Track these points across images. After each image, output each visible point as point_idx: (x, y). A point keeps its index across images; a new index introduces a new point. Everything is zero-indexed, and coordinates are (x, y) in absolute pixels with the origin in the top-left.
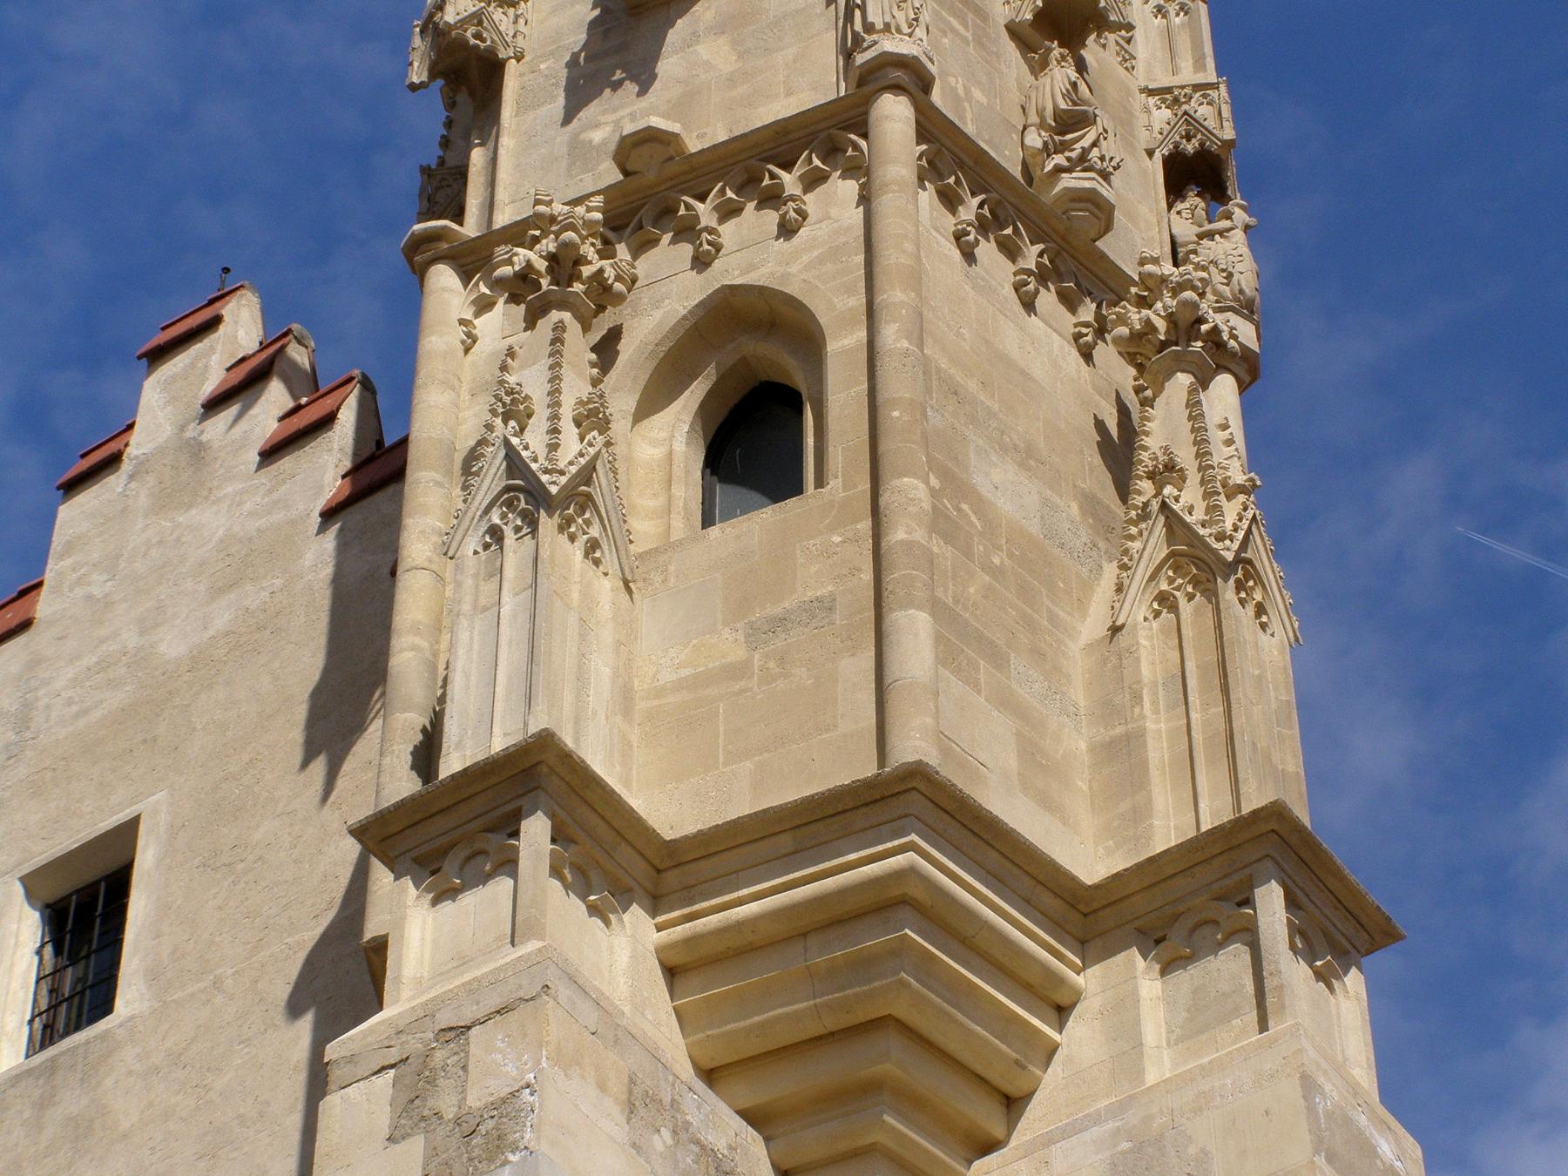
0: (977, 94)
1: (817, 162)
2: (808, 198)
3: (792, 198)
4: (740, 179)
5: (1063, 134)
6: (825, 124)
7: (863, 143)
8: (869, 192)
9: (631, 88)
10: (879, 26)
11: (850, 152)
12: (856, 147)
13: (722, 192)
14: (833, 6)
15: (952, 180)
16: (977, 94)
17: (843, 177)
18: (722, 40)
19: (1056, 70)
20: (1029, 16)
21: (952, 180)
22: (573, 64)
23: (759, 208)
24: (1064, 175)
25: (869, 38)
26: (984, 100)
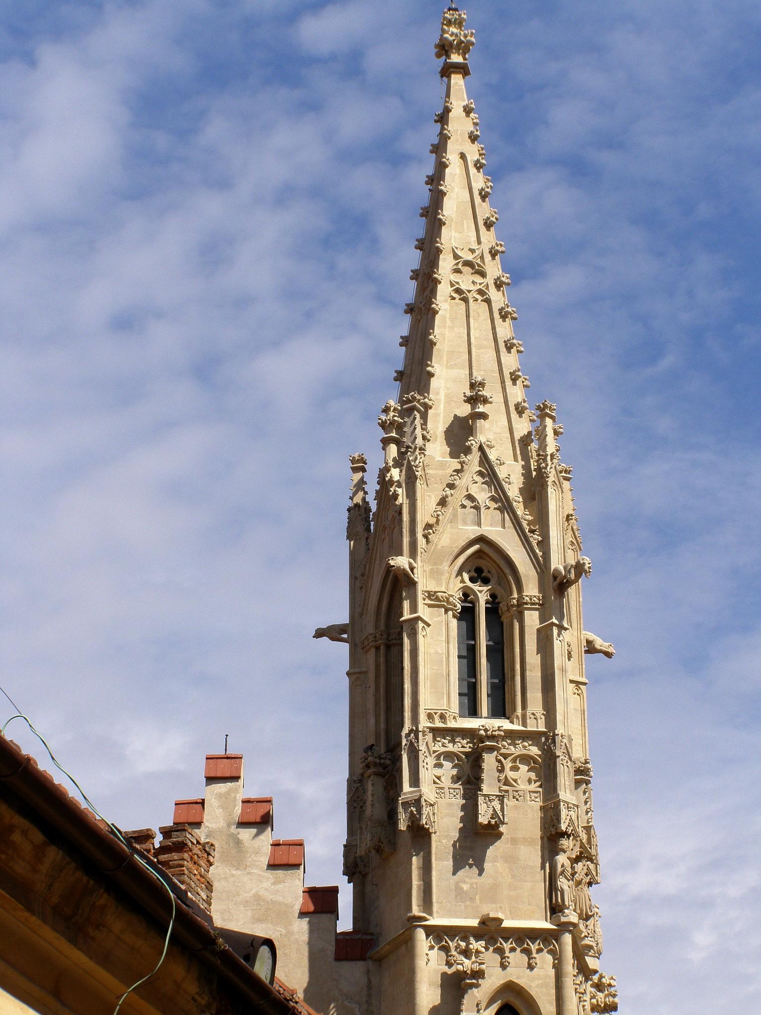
9: (475, 870)
12: (554, 946)
20: (574, 857)
22: (454, 845)
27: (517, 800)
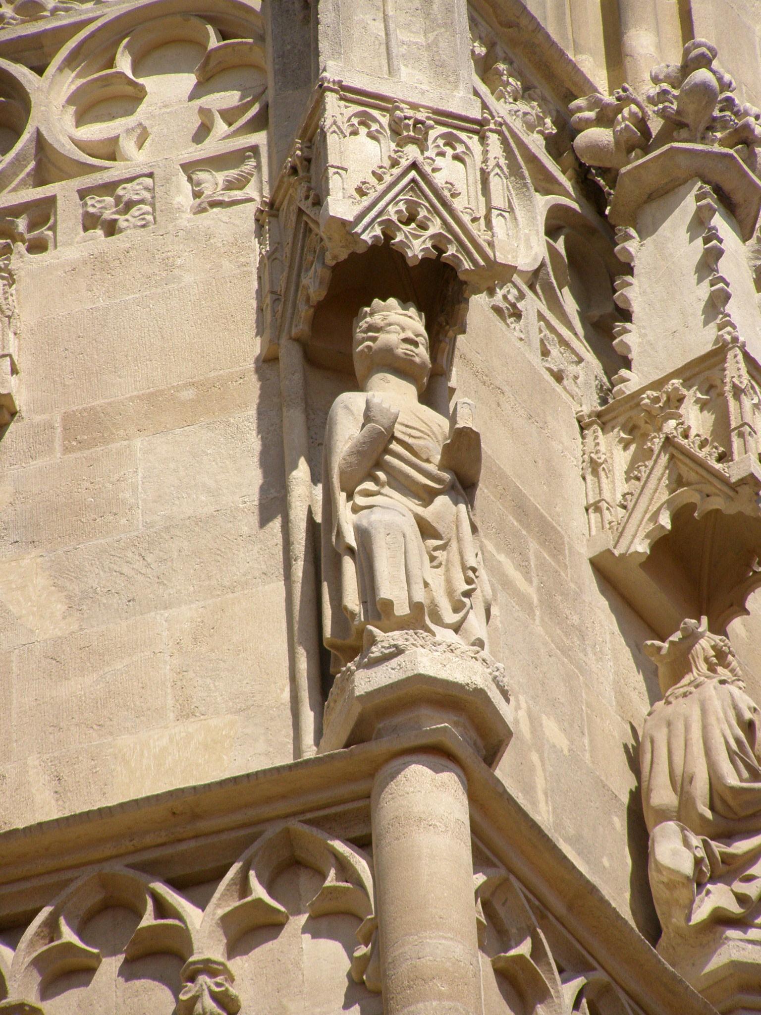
0: (551, 729)
1: (259, 891)
2: (239, 966)
3: (209, 968)
4: (95, 898)
5: (728, 837)
6: (282, 808)
7: (361, 865)
8: (382, 974)
10: (402, 609)
11: (331, 880)
12: (345, 870)
13: (51, 928)
14: (276, 524)
15: (524, 948)
16: (551, 729)
17: (314, 929)
18: (30, 559)
19: (711, 686)
20: (642, 547)
21: (524, 948)
23: (129, 971)
24: (732, 933)
25: (385, 639)
26: (563, 743)
27: (111, 229)
